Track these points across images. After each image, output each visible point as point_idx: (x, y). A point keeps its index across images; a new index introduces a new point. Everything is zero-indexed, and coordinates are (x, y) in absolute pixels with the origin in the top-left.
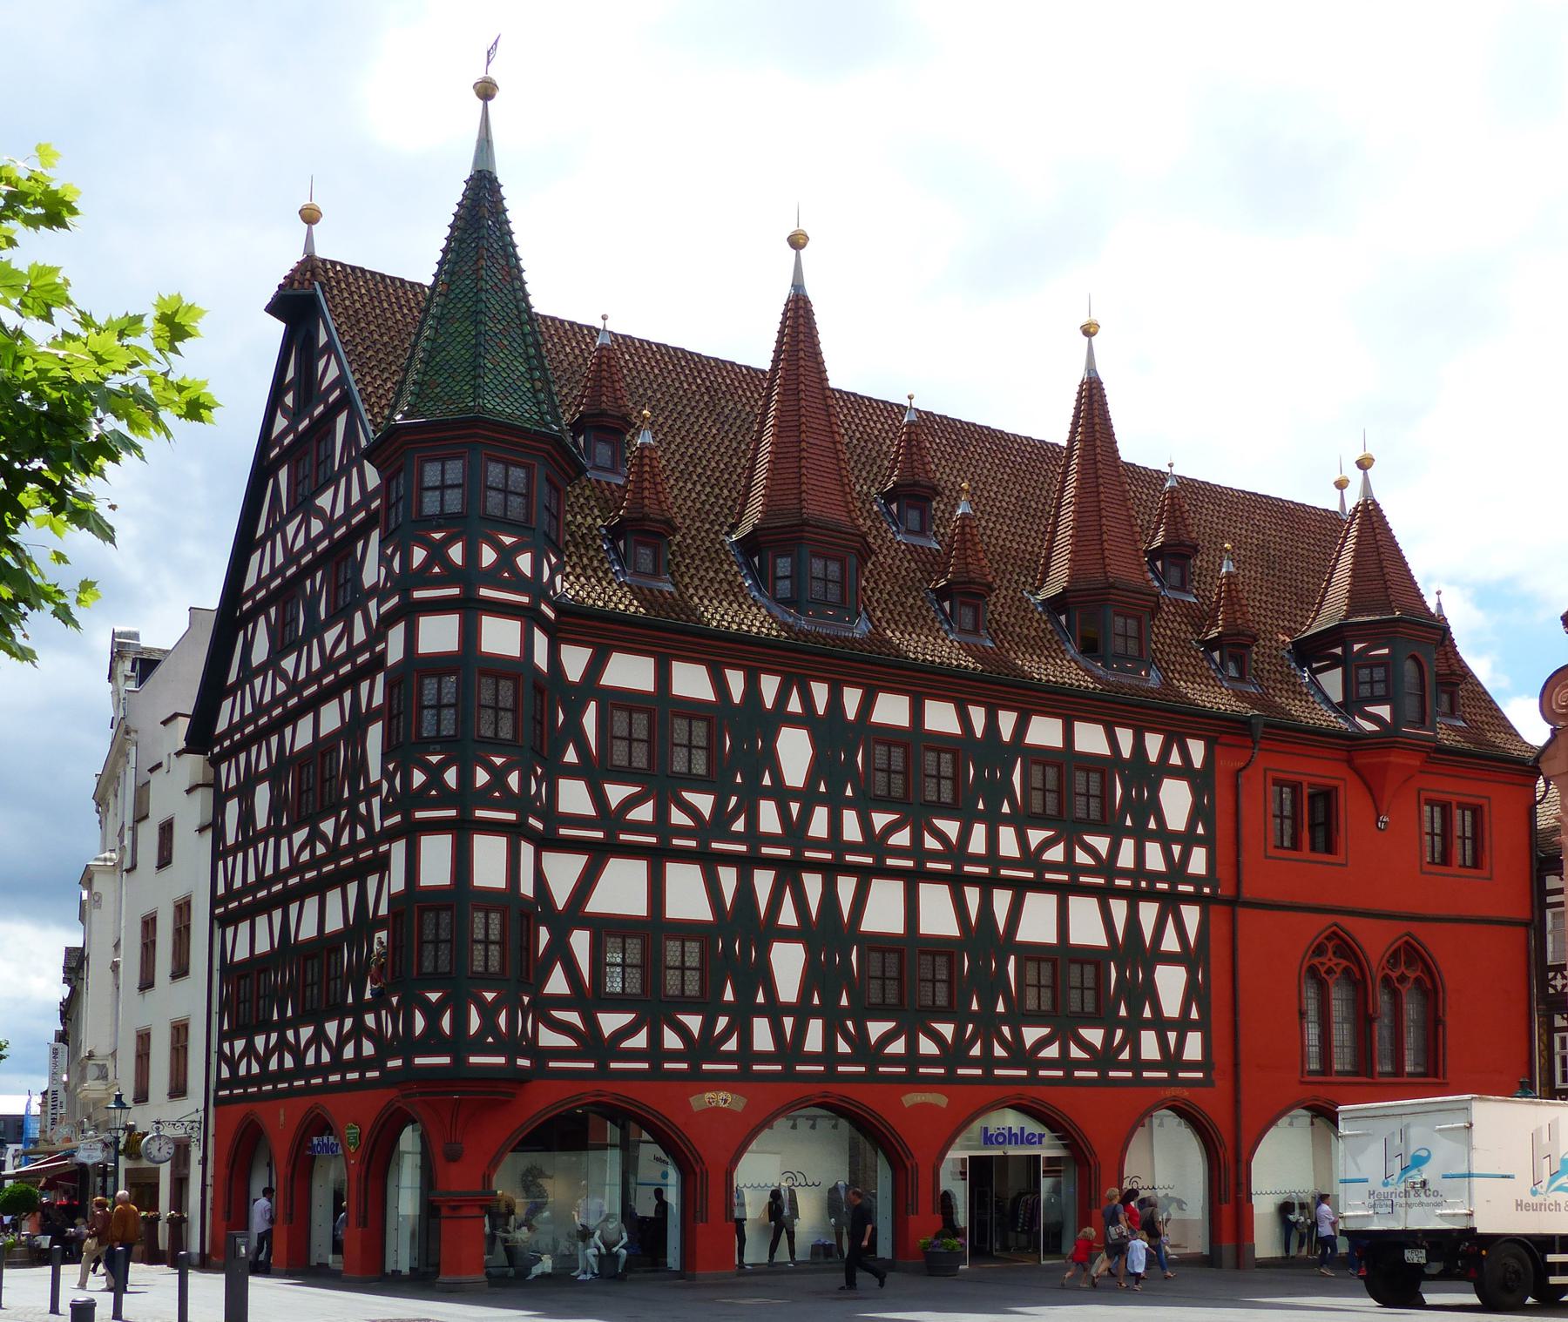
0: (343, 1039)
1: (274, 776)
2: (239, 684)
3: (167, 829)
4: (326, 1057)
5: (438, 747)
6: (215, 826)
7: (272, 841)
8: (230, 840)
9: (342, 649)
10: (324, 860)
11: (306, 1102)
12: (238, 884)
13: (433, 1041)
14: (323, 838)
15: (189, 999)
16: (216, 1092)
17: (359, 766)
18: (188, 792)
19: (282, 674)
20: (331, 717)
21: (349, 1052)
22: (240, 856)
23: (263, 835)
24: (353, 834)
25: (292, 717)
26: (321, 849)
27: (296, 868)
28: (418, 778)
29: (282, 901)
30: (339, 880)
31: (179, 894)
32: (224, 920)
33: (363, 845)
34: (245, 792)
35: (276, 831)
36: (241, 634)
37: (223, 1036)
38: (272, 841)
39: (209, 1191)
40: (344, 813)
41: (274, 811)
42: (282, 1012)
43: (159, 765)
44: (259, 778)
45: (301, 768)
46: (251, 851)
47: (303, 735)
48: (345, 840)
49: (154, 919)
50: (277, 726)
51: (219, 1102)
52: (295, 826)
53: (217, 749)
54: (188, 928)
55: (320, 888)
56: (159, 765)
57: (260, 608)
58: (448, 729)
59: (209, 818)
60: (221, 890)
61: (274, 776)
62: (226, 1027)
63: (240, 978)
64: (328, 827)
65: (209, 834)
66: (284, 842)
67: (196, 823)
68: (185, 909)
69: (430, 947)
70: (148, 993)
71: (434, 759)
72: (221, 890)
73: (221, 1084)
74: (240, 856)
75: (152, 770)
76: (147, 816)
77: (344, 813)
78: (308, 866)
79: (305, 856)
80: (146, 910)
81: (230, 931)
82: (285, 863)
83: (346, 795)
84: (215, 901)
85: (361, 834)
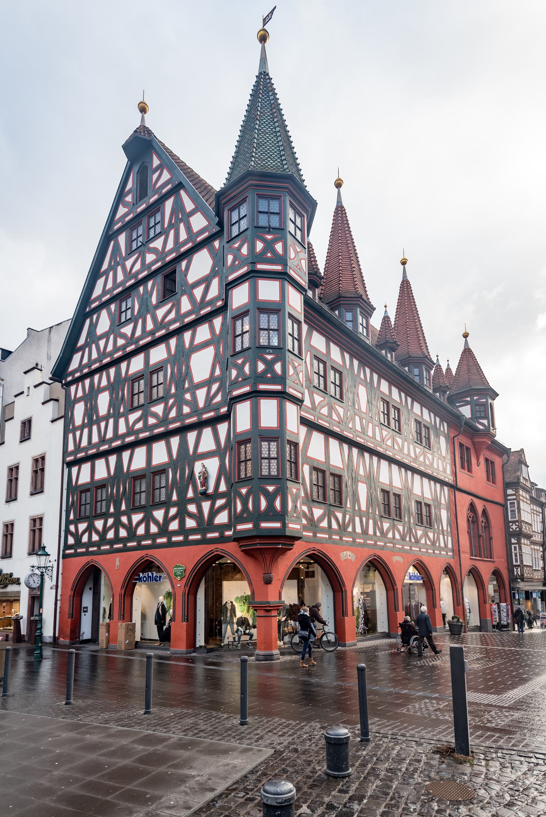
0: (167, 520)
1: (112, 388)
2: (87, 344)
3: (27, 425)
4: (154, 529)
5: (271, 351)
6: (67, 418)
7: (111, 421)
8: (78, 421)
9: (172, 315)
10: (155, 426)
11: (138, 554)
12: (84, 443)
13: (271, 514)
14: (155, 415)
15: (50, 505)
16: (64, 551)
17: (183, 376)
18: (43, 403)
19: (123, 336)
20: (158, 354)
21: (174, 526)
22: (86, 431)
23: (106, 418)
24: (180, 410)
25: (128, 356)
26: (152, 421)
27: (130, 431)
28: (261, 367)
29: (118, 451)
30: (166, 435)
31: (37, 453)
32: (71, 463)
33: (189, 416)
34: (90, 398)
35: (115, 414)
36: (88, 322)
37: (68, 522)
38: (111, 421)
39: (59, 602)
40: (171, 401)
41: (112, 404)
42: (117, 507)
43: (22, 393)
44: (101, 390)
45: (133, 383)
46: (95, 428)
47: (137, 364)
48: (173, 414)
49: (17, 468)
50: (116, 362)
51: (65, 556)
52: (133, 409)
53: (69, 379)
54: (43, 470)
55: (149, 441)
56: (22, 393)
57: (105, 305)
58: (275, 342)
59: (62, 414)
60: (71, 447)
61: (112, 388)
62: (72, 517)
63: (82, 492)
64: (159, 409)
65: (61, 422)
66: (122, 421)
67: (51, 418)
68: (40, 460)
69: (266, 461)
70: (12, 504)
71: (269, 357)
72: (71, 447)
73: (67, 547)
74: (86, 431)
75: (16, 396)
76: (12, 418)
77: (171, 401)
78: (141, 431)
79: (140, 425)
80: (12, 462)
81: (75, 470)
82: (122, 429)
83: (173, 391)
84: (65, 452)
85: (186, 410)
